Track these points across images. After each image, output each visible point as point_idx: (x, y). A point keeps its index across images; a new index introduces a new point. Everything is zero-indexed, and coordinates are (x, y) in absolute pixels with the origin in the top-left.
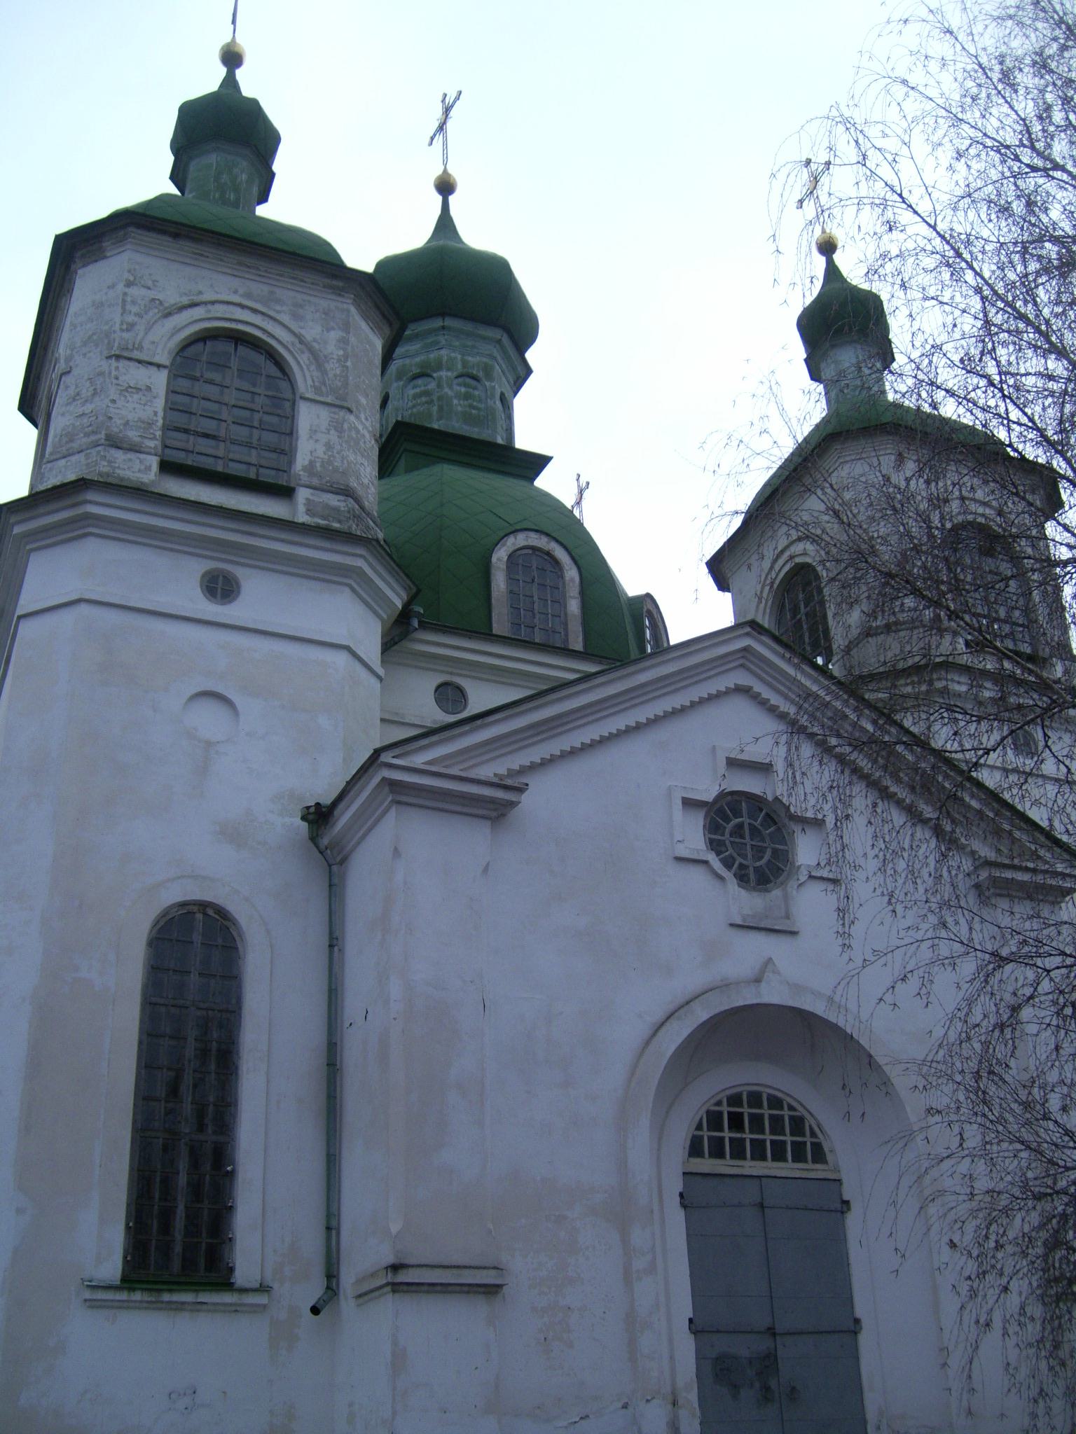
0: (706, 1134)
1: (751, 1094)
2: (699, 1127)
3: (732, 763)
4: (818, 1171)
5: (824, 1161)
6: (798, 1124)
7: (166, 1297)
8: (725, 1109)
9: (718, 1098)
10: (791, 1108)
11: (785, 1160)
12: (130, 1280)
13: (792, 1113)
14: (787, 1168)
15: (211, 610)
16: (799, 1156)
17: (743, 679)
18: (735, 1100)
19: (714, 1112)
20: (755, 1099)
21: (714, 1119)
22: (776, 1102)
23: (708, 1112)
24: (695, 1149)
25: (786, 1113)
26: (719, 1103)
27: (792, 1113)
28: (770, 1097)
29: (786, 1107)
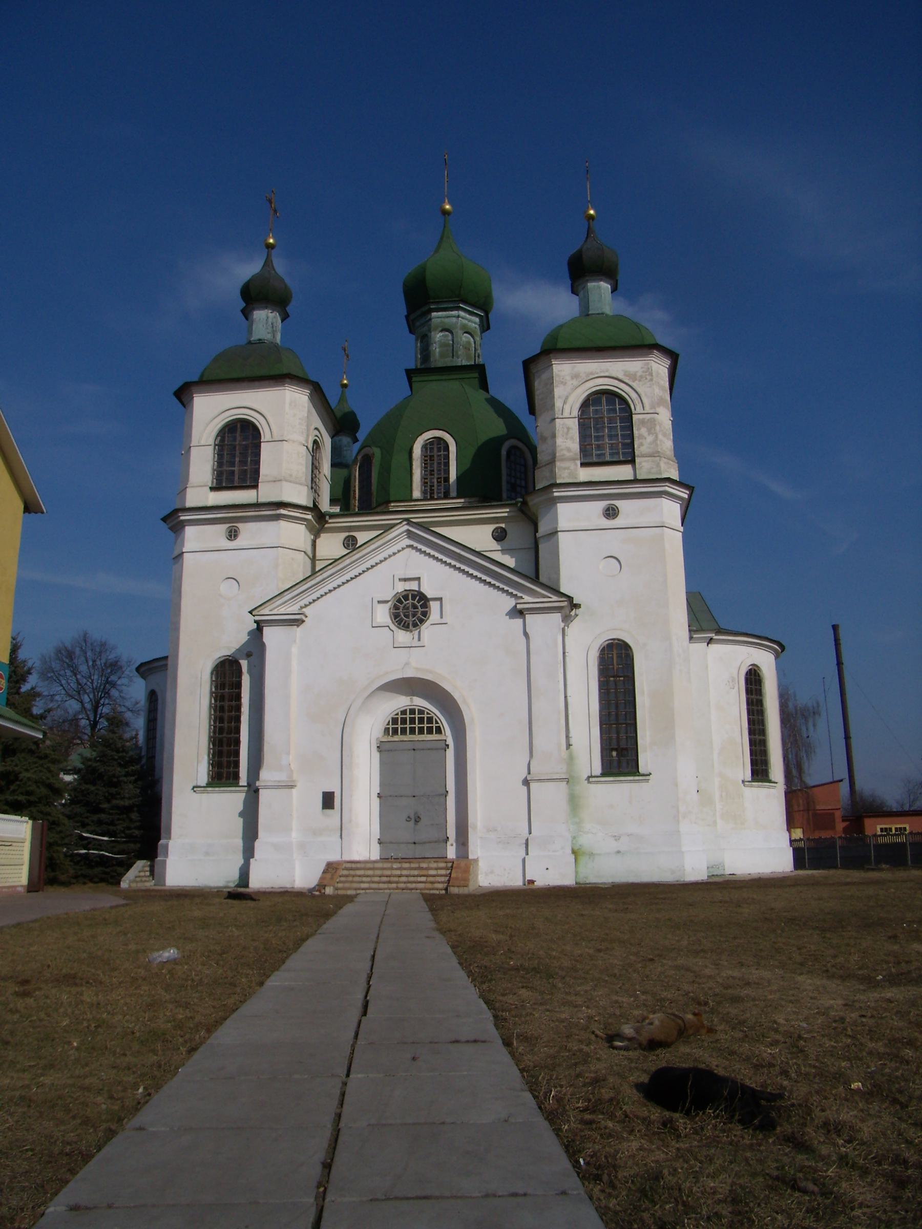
0: (391, 726)
1: (410, 709)
2: (388, 724)
4: (434, 737)
6: (430, 720)
7: (222, 789)
8: (399, 716)
9: (395, 713)
10: (428, 713)
11: (432, 733)
12: (209, 785)
13: (428, 716)
14: (426, 737)
16: (430, 731)
18: (404, 712)
19: (395, 718)
20: (412, 711)
21: (395, 721)
22: (421, 712)
23: (392, 718)
24: (387, 730)
25: (425, 716)
26: (397, 714)
27: (428, 716)
28: (418, 709)
29: (426, 713)
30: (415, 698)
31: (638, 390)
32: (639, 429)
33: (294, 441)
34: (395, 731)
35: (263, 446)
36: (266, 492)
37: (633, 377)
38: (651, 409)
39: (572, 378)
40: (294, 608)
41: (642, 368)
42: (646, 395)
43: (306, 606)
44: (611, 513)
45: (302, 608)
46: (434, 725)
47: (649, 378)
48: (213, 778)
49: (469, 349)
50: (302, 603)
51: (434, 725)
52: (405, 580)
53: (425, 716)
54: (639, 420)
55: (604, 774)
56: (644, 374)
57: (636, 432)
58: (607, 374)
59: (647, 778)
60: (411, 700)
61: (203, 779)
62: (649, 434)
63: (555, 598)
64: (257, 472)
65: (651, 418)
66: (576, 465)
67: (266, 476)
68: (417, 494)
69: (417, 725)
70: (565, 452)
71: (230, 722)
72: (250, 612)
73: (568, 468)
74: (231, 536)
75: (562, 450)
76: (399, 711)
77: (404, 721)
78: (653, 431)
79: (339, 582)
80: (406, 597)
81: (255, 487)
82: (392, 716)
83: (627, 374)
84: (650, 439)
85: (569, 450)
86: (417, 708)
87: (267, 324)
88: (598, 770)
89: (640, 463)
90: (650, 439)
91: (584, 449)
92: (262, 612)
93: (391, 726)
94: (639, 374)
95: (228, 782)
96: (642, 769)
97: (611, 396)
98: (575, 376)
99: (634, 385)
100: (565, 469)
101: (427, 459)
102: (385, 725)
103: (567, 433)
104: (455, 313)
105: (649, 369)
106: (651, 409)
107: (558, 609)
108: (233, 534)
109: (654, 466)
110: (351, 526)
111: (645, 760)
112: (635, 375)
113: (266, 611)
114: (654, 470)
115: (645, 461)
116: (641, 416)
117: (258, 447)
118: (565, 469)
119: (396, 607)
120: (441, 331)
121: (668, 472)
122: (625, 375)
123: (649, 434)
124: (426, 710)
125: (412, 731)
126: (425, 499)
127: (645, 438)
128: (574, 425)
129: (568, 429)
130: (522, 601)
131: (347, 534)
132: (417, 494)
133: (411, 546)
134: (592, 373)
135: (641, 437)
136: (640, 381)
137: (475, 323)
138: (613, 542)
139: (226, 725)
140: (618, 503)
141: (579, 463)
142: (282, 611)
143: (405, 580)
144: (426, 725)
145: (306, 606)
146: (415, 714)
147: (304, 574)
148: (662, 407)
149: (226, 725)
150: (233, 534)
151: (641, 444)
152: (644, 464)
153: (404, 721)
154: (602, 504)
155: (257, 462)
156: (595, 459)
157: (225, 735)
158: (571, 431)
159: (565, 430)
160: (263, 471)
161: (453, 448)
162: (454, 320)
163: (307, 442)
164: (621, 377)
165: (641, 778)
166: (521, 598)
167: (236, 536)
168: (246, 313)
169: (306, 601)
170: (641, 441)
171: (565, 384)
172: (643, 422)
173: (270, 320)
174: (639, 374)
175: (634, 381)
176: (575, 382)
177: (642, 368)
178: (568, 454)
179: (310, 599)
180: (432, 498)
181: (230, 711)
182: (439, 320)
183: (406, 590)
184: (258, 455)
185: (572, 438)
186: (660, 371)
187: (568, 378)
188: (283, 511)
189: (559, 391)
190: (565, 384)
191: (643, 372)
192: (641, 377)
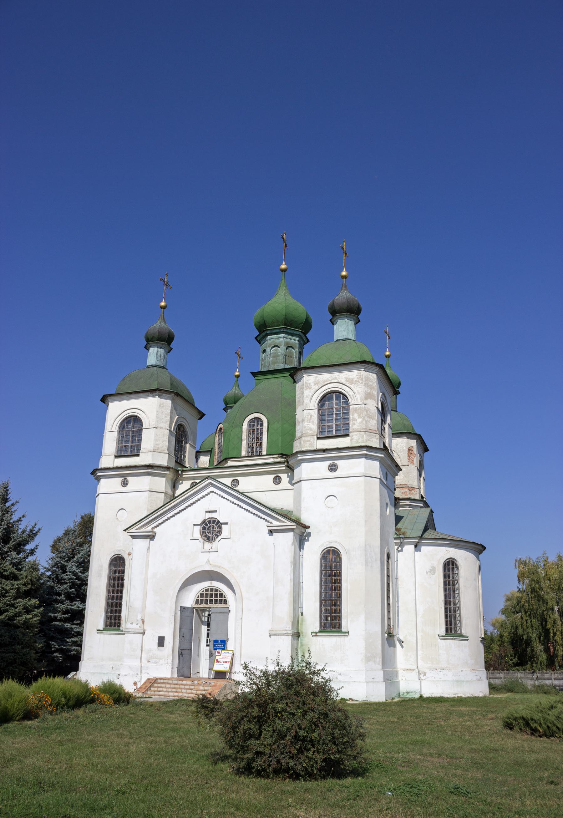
0: (199, 598)
2: (198, 597)
3: (206, 512)
4: (223, 605)
5: (227, 603)
6: (221, 595)
8: (204, 593)
10: (220, 591)
11: (222, 603)
12: (104, 629)
15: (124, 489)
17: (212, 489)
18: (207, 590)
20: (212, 590)
21: (202, 595)
22: (216, 590)
23: (201, 594)
26: (203, 591)
30: (213, 582)
31: (353, 389)
32: (353, 415)
33: (161, 428)
34: (202, 602)
35: (144, 431)
36: (143, 459)
37: (351, 381)
38: (361, 401)
39: (315, 385)
40: (149, 528)
41: (357, 376)
42: (358, 393)
43: (156, 527)
44: (333, 468)
45: (153, 528)
46: (223, 599)
47: (360, 381)
48: (106, 625)
49: (291, 357)
50: (153, 526)
51: (223, 599)
52: (209, 512)
53: (219, 593)
54: (353, 408)
55: (320, 632)
56: (358, 379)
57: (351, 417)
58: (335, 381)
59: (347, 634)
60: (211, 584)
61: (101, 626)
62: (359, 418)
63: (289, 523)
64: (139, 446)
65: (361, 407)
66: (314, 438)
67: (145, 448)
68: (244, 453)
69: (214, 598)
70: (309, 431)
71: (117, 593)
72: (125, 530)
73: (309, 441)
74: (124, 484)
75: (307, 429)
76: (204, 589)
77: (216, 595)
78: (361, 416)
79: (173, 513)
80: (210, 522)
81: (138, 455)
82: (200, 592)
83: (348, 380)
84: (359, 420)
85: (310, 429)
86: (214, 588)
87: (157, 355)
88: (317, 629)
89: (352, 436)
90: (359, 420)
91: (321, 429)
92: (131, 531)
93: (199, 598)
94: (354, 380)
95: (115, 628)
96: (344, 629)
97: (339, 395)
98: (317, 383)
99: (351, 386)
100: (307, 441)
101: (251, 430)
102: (196, 598)
103: (310, 419)
104: (282, 335)
105: (361, 376)
106: (361, 401)
107: (292, 530)
108: (125, 483)
110: (194, 477)
111: (346, 623)
112: (353, 380)
113: (133, 530)
114: (360, 440)
115: (355, 435)
116: (355, 406)
117: (140, 431)
118: (307, 441)
119: (204, 528)
120: (274, 347)
121: (370, 440)
122: (346, 381)
123: (359, 418)
124: (219, 590)
125: (211, 601)
126: (248, 457)
127: (357, 420)
128: (315, 414)
129: (311, 416)
130: (271, 525)
131: (193, 481)
132: (244, 453)
133: (213, 492)
134: (326, 381)
135: (355, 419)
136: (355, 384)
137: (295, 340)
138: (332, 486)
139: (116, 595)
140: (337, 462)
141: (315, 437)
142: (142, 530)
143: (209, 512)
144: (218, 599)
145: (156, 527)
146: (213, 591)
147: (148, 510)
148: (369, 400)
149: (116, 595)
150: (125, 483)
151: (354, 424)
152: (354, 436)
153: (207, 595)
154: (328, 463)
155: (140, 440)
156: (326, 435)
157: (114, 601)
158: (313, 418)
159: (309, 417)
160: (143, 446)
161: (265, 424)
162: (281, 340)
163: (170, 427)
164: (343, 382)
165: (342, 634)
166: (271, 523)
167: (127, 484)
168: (147, 348)
169: (155, 524)
170: (354, 422)
171: (310, 388)
172: (356, 410)
173: (159, 353)
174: (354, 380)
175: (351, 385)
176: (317, 387)
177: (357, 376)
178: (310, 432)
179: (157, 523)
180: (252, 456)
181: (118, 587)
182: (272, 340)
183: (209, 518)
184: (140, 435)
185: (313, 422)
186: (369, 377)
187: (312, 384)
189: (307, 393)
190: (310, 388)
191: (358, 378)
192: (356, 381)
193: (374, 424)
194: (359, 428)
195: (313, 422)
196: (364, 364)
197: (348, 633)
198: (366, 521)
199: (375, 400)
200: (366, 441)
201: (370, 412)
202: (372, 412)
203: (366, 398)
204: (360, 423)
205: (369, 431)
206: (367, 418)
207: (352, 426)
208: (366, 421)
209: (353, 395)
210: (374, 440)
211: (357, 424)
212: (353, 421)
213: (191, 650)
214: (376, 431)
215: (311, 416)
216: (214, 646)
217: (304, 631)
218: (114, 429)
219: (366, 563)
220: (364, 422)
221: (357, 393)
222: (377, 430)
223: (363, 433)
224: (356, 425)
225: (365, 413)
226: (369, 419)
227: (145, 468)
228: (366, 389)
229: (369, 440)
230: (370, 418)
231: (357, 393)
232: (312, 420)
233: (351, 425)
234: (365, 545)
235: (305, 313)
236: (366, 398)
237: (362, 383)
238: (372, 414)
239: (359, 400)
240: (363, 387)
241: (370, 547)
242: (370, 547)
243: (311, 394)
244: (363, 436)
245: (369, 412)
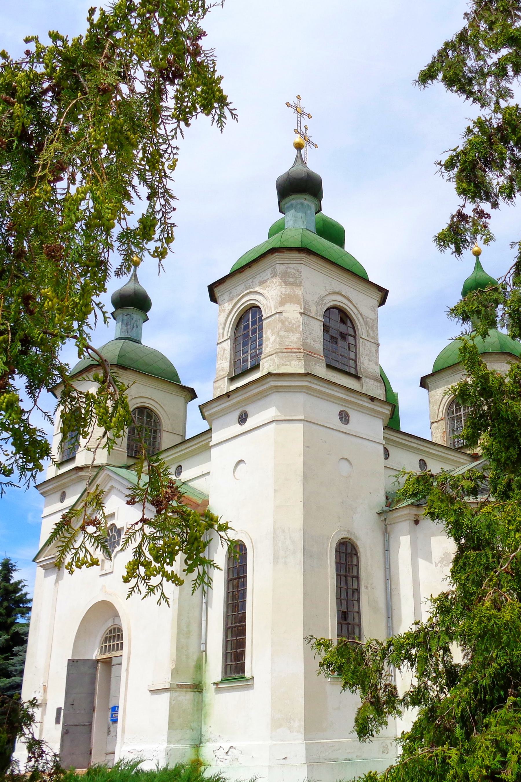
32: (266, 334)
41: (271, 274)
57: (264, 336)
66: (224, 381)
73: (219, 387)
75: (220, 371)
85: (223, 369)
90: (272, 338)
96: (248, 675)
109: (271, 365)
121: (286, 365)
141: (226, 379)
152: (266, 364)
158: (226, 352)
159: (222, 352)
172: (269, 324)
177: (271, 274)
186: (289, 270)
188: (81, 474)
193: (295, 340)
194: (272, 349)
195: (226, 357)
196: (276, 254)
197: (253, 678)
198: (275, 491)
199: (299, 303)
200: (279, 367)
201: (290, 323)
202: (293, 321)
203: (282, 303)
204: (272, 344)
205: (285, 351)
206: (282, 333)
207: (265, 349)
208: (281, 337)
209: (267, 304)
210: (294, 363)
211: (270, 346)
212: (266, 342)
213: (91, 724)
214: (298, 349)
215: (224, 350)
216: (112, 714)
217: (207, 682)
218: (59, 431)
219: (276, 559)
220: (278, 339)
221: (270, 299)
222: (301, 347)
223: (274, 356)
224: (269, 347)
225: (279, 325)
226: (287, 334)
227: (75, 472)
228: (283, 290)
229: (283, 365)
230: (288, 331)
231: (270, 299)
232: (224, 356)
233: (263, 350)
234: (274, 530)
235: (322, 222)
236: (282, 303)
237: (276, 282)
238: (293, 324)
239: (273, 309)
240: (278, 288)
241: (283, 531)
242: (283, 531)
243: (224, 320)
244: (274, 361)
245: (287, 323)
